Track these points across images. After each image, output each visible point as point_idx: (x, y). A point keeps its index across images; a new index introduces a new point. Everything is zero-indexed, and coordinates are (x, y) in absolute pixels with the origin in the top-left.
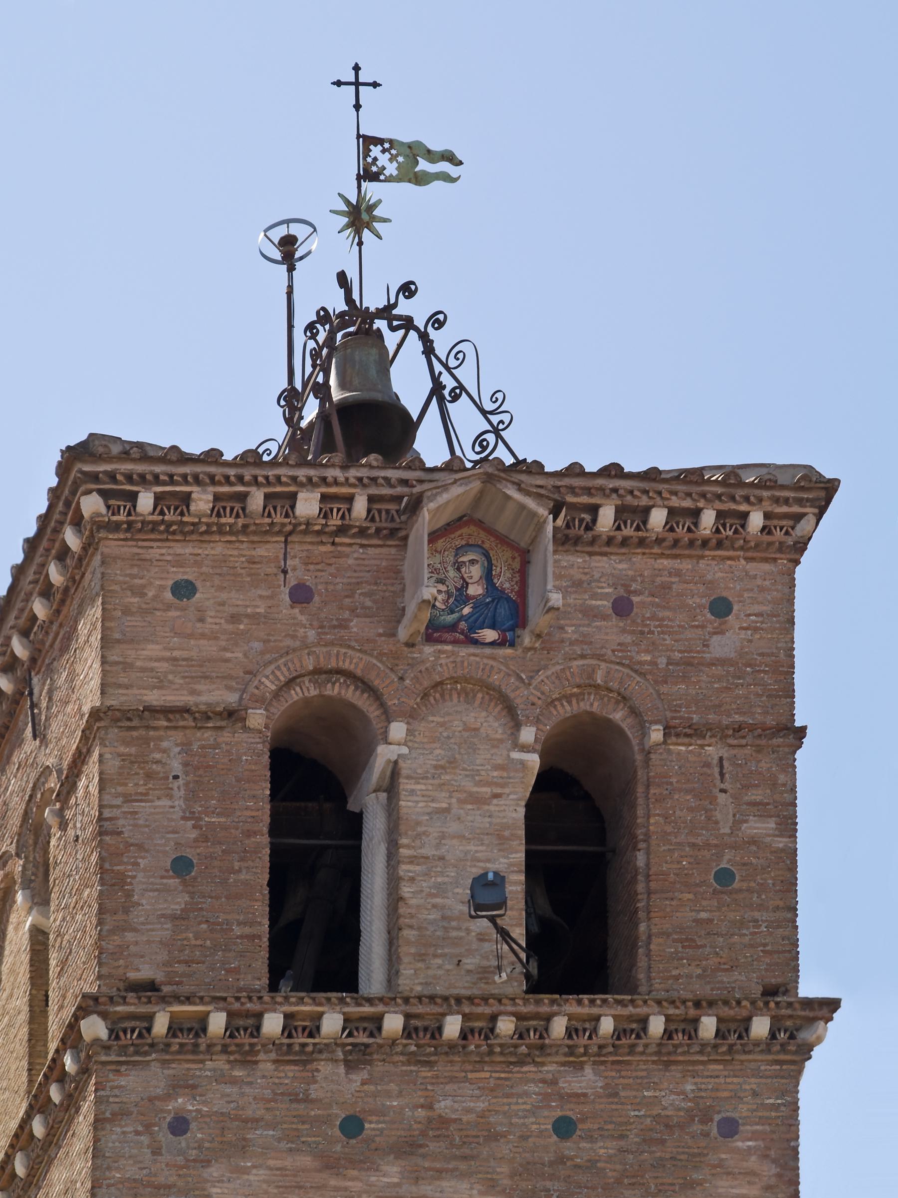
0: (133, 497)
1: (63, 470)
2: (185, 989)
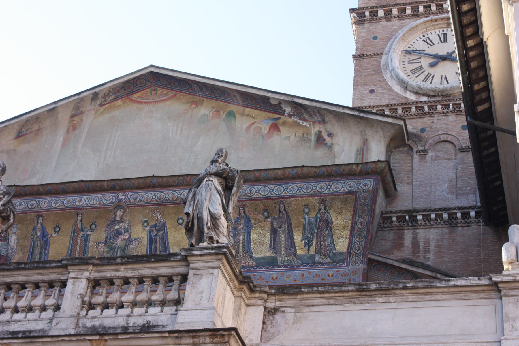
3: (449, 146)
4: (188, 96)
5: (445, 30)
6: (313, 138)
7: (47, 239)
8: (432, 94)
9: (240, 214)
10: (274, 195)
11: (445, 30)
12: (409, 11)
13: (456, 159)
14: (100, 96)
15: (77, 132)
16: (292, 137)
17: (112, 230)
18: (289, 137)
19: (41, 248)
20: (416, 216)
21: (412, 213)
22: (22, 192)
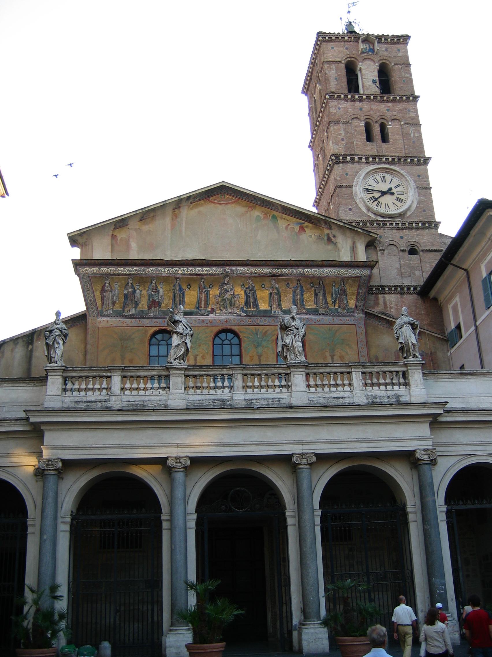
0: (325, 38)
1: (317, 34)
2: (338, 93)
3: (394, 247)
4: (246, 203)
5: (384, 174)
6: (326, 238)
7: (183, 292)
8: (384, 216)
9: (297, 284)
10: (317, 275)
11: (384, 175)
12: (364, 160)
13: (399, 256)
14: (192, 198)
15: (178, 220)
16: (313, 236)
17: (222, 289)
18: (311, 235)
19: (180, 297)
20: (385, 288)
21: (383, 287)
22: (166, 263)
